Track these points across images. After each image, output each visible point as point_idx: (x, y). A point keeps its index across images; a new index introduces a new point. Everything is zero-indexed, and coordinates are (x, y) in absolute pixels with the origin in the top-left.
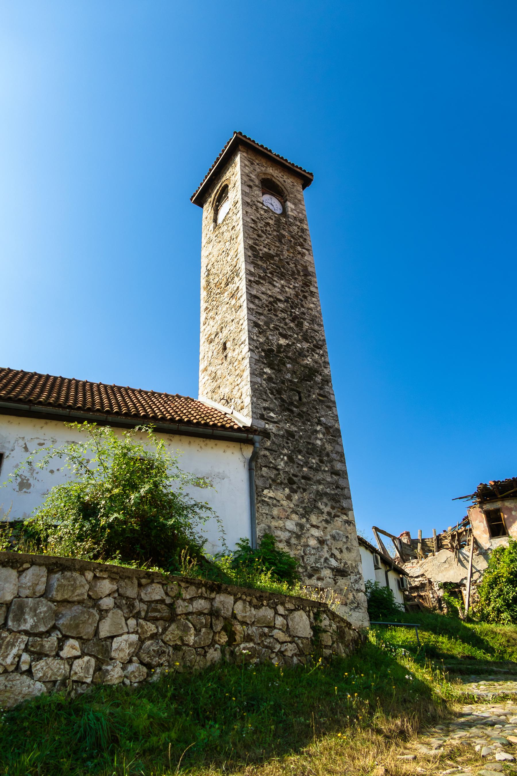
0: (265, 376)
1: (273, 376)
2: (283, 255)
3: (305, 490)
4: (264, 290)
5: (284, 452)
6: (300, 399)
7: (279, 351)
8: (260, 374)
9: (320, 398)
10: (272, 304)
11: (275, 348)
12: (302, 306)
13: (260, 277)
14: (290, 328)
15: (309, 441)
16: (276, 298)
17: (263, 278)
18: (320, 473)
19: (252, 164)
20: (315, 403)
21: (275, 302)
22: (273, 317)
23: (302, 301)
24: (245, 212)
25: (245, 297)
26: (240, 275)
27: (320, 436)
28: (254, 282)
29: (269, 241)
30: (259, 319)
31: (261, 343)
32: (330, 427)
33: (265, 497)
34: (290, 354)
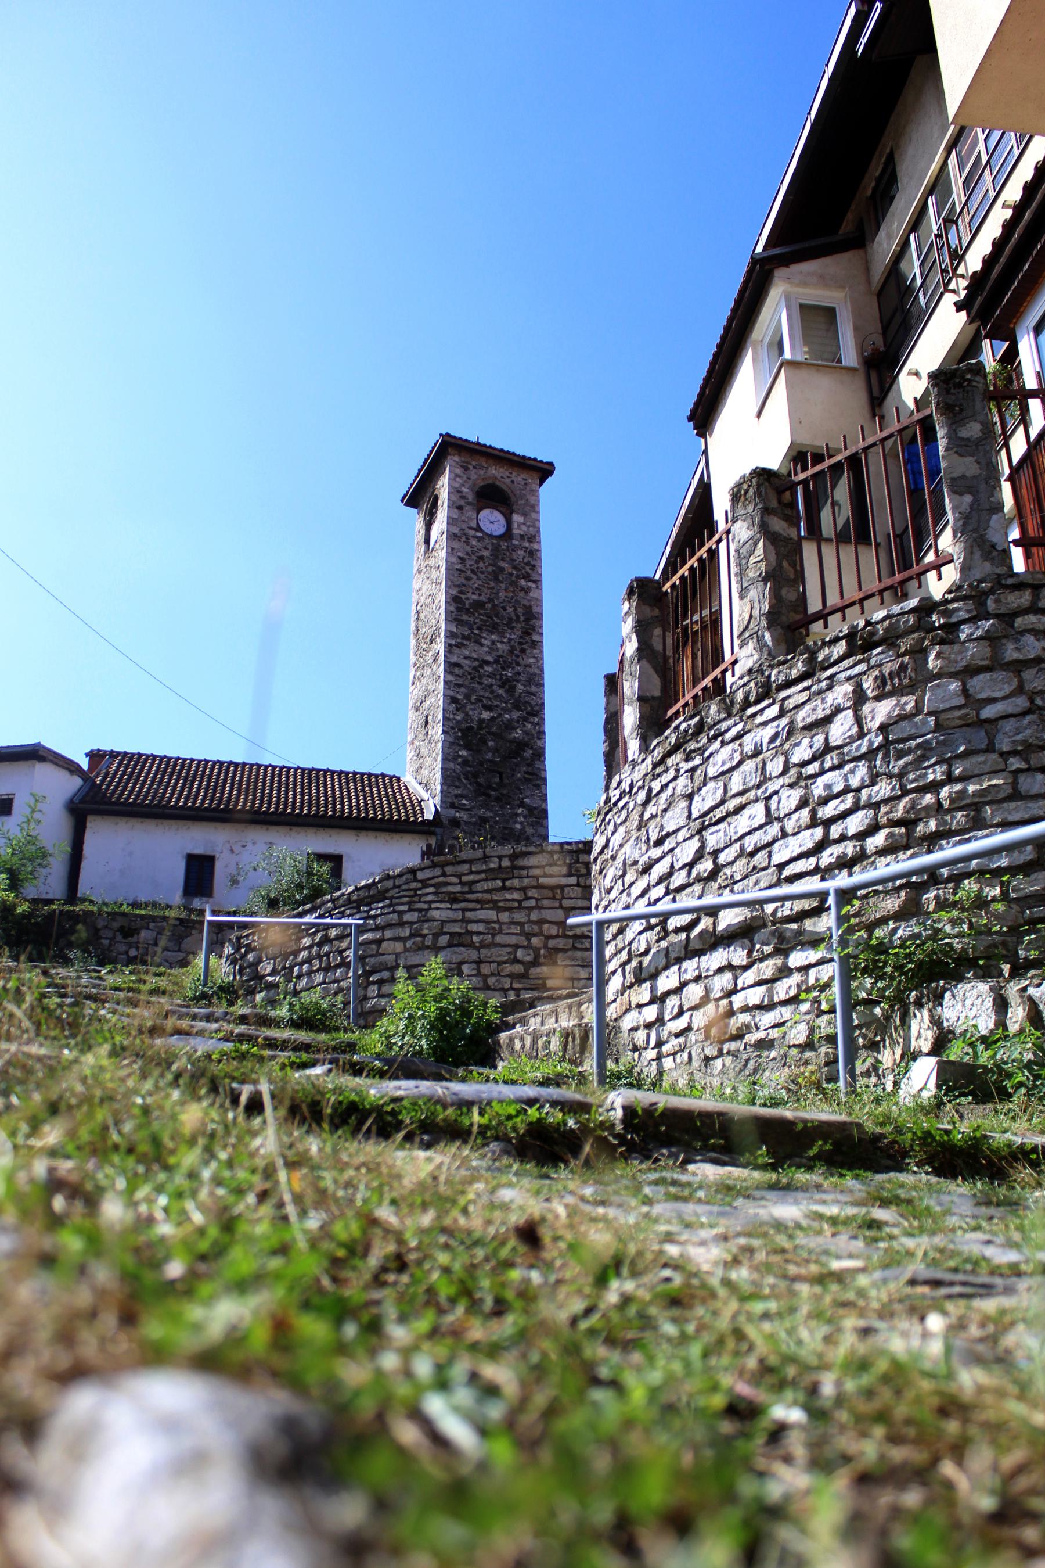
4: (467, 653)
7: (480, 728)
11: (475, 725)
12: (518, 664)
13: (464, 637)
14: (499, 696)
19: (466, 469)
31: (458, 722)
34: (494, 729)
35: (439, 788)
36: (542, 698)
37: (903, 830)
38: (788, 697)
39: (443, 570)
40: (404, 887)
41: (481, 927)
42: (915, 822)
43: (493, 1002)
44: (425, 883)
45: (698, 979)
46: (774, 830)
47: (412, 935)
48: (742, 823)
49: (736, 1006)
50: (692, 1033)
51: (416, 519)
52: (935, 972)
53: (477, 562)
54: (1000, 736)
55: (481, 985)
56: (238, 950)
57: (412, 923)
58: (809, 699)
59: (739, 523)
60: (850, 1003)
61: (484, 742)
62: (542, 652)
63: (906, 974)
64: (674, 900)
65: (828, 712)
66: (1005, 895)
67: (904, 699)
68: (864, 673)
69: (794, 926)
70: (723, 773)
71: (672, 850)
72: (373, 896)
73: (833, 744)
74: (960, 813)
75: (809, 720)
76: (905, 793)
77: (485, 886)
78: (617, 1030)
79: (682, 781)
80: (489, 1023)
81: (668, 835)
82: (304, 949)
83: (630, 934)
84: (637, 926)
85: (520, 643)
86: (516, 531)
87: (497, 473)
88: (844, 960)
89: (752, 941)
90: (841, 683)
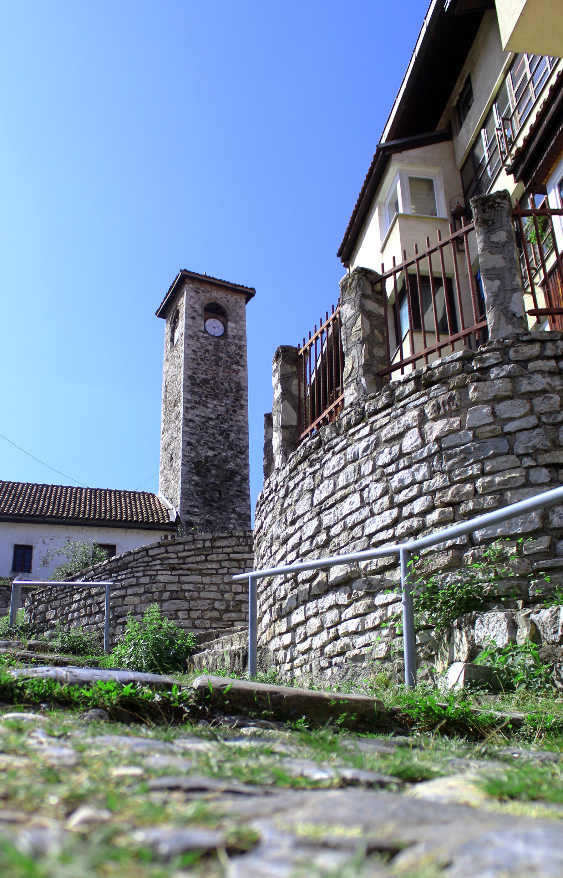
1: (200, 482)
2: (218, 377)
4: (198, 412)
7: (206, 462)
11: (203, 460)
12: (231, 420)
13: (196, 402)
14: (218, 441)
19: (197, 293)
21: (207, 421)
22: (204, 434)
23: (231, 415)
27: (234, 521)
29: (206, 367)
31: (192, 458)
34: (216, 463)
35: (179, 501)
36: (247, 442)
37: (451, 509)
38: (376, 421)
39: (182, 359)
40: (140, 560)
41: (191, 587)
42: (459, 504)
43: (192, 634)
44: (154, 558)
45: (316, 615)
46: (366, 511)
47: (145, 592)
48: (345, 507)
49: (340, 632)
50: (302, 649)
51: (165, 325)
52: (471, 605)
53: (204, 353)
54: (517, 444)
55: (190, 625)
56: (33, 603)
57: (145, 584)
58: (389, 422)
59: (346, 306)
60: (413, 630)
61: (209, 471)
62: (247, 412)
63: (450, 607)
64: (302, 561)
65: (402, 430)
66: (519, 552)
67: (452, 420)
68: (426, 403)
69: (378, 577)
70: (333, 474)
71: (301, 527)
72: (120, 567)
73: (404, 452)
74: (490, 497)
75: (389, 436)
76: (453, 483)
77: (193, 559)
78: (266, 651)
79: (307, 480)
80: (188, 649)
81: (299, 517)
82: (75, 602)
83: (275, 586)
84: (279, 579)
85: (233, 406)
86: (230, 333)
87: (218, 295)
88: (409, 598)
89: (351, 587)
90: (410, 410)
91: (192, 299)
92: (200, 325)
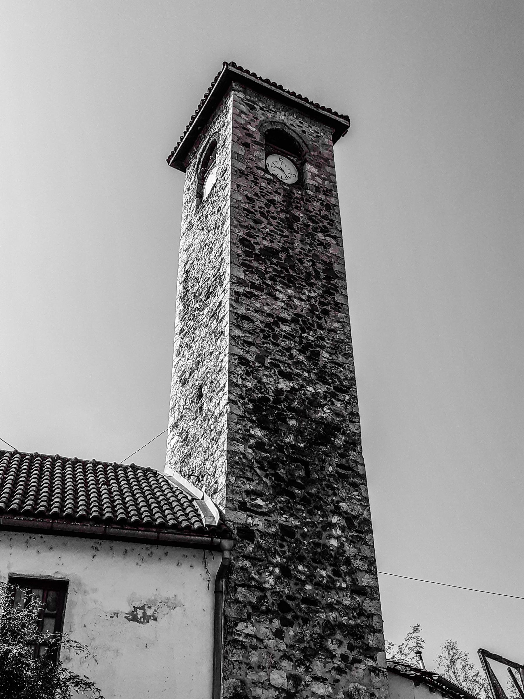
0: (252, 441)
1: (265, 440)
2: (293, 249)
3: (306, 621)
4: (259, 305)
5: (275, 561)
6: (307, 472)
7: (277, 401)
8: (243, 438)
9: (340, 471)
10: (270, 328)
11: (270, 396)
12: (320, 327)
13: (253, 286)
14: (298, 363)
15: (317, 541)
16: (277, 317)
17: (259, 288)
18: (333, 592)
19: (252, 108)
20: (331, 479)
22: (271, 347)
24: (235, 187)
25: (227, 319)
26: (225, 283)
28: (244, 294)
29: (272, 228)
30: (248, 352)
31: (249, 390)
32: (354, 517)
33: (239, 635)
35: (222, 480)
53: (266, 205)
62: (348, 317)
85: (321, 303)
91: (243, 116)
92: (260, 160)
